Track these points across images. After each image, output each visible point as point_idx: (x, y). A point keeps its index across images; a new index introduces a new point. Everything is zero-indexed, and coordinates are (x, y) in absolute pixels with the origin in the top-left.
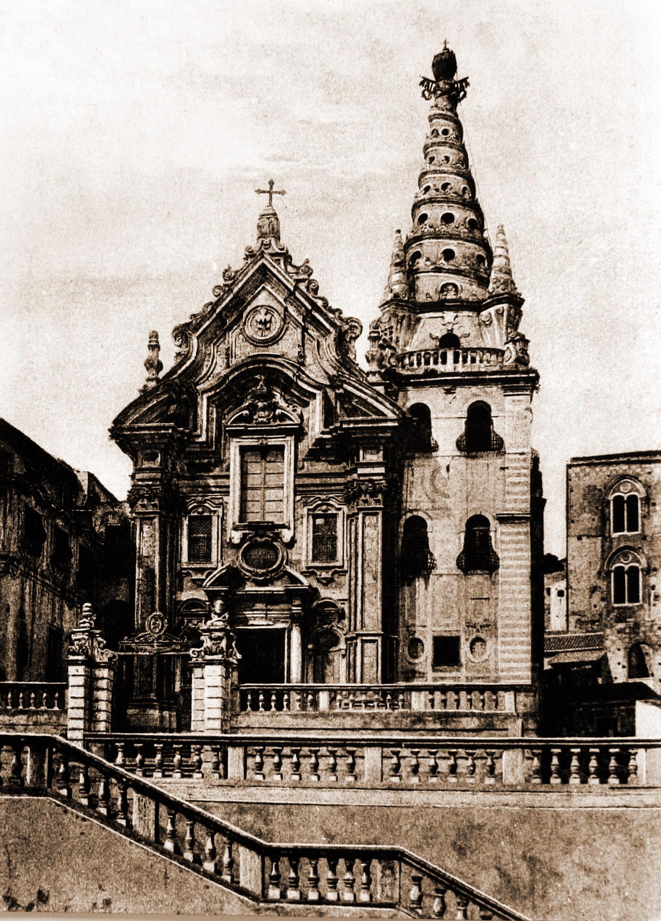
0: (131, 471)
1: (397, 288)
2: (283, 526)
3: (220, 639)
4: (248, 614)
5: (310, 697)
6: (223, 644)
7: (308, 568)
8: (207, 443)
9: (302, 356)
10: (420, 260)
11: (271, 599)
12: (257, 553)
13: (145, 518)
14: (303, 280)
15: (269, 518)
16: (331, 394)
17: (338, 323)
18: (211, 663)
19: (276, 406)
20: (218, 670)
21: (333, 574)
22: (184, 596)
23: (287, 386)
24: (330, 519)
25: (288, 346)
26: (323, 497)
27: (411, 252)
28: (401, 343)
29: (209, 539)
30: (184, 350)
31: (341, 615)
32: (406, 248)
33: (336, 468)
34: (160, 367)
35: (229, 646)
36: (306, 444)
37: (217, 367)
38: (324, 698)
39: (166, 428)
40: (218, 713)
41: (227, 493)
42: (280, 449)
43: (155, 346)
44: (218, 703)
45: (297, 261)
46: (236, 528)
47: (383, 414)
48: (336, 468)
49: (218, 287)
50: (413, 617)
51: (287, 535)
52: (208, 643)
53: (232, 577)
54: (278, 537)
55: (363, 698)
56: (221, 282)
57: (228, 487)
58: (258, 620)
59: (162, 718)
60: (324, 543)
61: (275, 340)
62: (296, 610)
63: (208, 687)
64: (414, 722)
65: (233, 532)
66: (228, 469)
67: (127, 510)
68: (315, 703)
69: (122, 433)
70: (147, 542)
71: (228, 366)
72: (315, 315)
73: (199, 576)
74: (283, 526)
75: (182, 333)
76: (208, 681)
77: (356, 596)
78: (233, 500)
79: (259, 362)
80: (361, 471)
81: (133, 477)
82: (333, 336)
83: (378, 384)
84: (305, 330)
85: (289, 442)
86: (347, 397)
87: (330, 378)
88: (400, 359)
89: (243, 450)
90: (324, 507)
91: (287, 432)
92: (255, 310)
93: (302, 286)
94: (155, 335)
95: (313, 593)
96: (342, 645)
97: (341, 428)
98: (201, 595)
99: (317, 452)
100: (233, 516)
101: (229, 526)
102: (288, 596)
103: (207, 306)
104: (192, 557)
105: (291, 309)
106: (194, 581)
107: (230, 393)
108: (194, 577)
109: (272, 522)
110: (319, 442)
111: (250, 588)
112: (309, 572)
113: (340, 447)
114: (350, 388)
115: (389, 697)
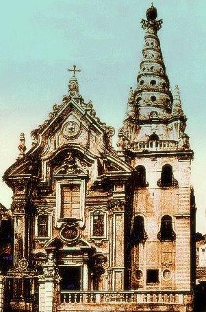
1: (130, 114)
2: (80, 220)
3: (52, 270)
4: (64, 259)
5: (92, 297)
6: (53, 273)
8: (47, 183)
9: (88, 144)
11: (75, 253)
12: (69, 232)
13: (18, 217)
14: (89, 110)
15: (73, 217)
16: (101, 161)
18: (48, 281)
19: (76, 167)
20: (52, 284)
22: (36, 251)
23: (82, 157)
24: (101, 217)
25: (82, 140)
27: (137, 97)
28: (132, 138)
29: (47, 226)
30: (36, 141)
31: (106, 260)
32: (135, 95)
33: (103, 194)
34: (25, 149)
35: (56, 274)
36: (90, 183)
37: (50, 149)
38: (98, 297)
39: (28, 176)
40: (51, 304)
42: (78, 186)
44: (52, 299)
46: (59, 221)
47: (122, 169)
48: (103, 194)
50: (137, 260)
51: (81, 224)
52: (46, 272)
53: (57, 243)
54: (77, 225)
55: (116, 297)
58: (69, 262)
59: (26, 306)
60: (98, 229)
61: (76, 137)
62: (86, 257)
63: (46, 292)
64: (138, 308)
66: (55, 195)
67: (11, 213)
68: (94, 299)
69: (8, 179)
70: (19, 227)
71: (55, 148)
72: (94, 125)
73: (42, 242)
74: (80, 220)
75: (35, 133)
76: (46, 289)
77: (113, 251)
78: (58, 209)
79: (69, 147)
80: (114, 195)
81: (13, 198)
82: (102, 135)
83: (122, 156)
84: (89, 132)
86: (108, 162)
87: (101, 154)
88: (132, 145)
89: (62, 186)
91: (82, 178)
92: (68, 123)
93: (88, 113)
95: (92, 251)
96: (106, 273)
98: (43, 251)
99: (95, 187)
100: (57, 215)
102: (82, 252)
103: (46, 121)
104: (40, 233)
105: (84, 123)
106: (40, 245)
107: (56, 161)
110: (96, 183)
111: (65, 248)
112: (92, 241)
113: (105, 185)
114: (109, 158)
115: (127, 297)
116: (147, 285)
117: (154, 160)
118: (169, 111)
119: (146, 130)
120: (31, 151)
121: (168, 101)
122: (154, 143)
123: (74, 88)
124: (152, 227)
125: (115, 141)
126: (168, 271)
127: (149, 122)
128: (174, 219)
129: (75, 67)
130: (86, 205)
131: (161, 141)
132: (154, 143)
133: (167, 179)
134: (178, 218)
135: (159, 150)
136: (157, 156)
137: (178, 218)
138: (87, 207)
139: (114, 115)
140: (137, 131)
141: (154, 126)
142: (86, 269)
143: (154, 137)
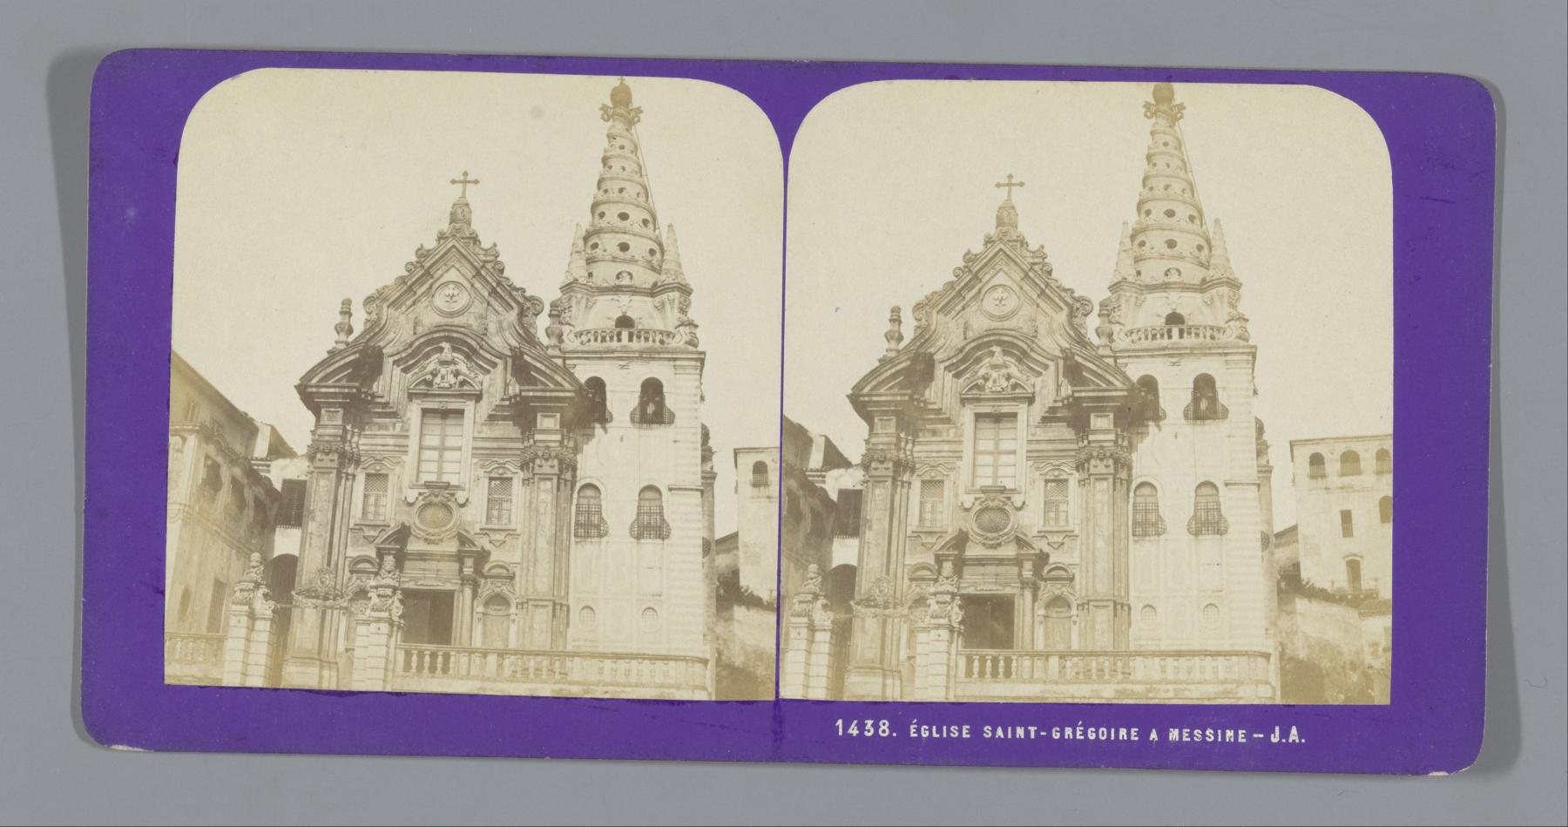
2: (458, 487)
15: (446, 478)
17: (521, 300)
24: (506, 481)
34: (350, 331)
51: (461, 496)
56: (414, 259)
72: (501, 290)
80: (537, 437)
87: (512, 349)
100: (408, 475)
117: (622, 367)
118: (657, 270)
122: (625, 335)
123: (460, 216)
124: (619, 510)
125: (542, 322)
128: (664, 491)
130: (474, 455)
132: (625, 335)
133: (652, 406)
143: (625, 322)
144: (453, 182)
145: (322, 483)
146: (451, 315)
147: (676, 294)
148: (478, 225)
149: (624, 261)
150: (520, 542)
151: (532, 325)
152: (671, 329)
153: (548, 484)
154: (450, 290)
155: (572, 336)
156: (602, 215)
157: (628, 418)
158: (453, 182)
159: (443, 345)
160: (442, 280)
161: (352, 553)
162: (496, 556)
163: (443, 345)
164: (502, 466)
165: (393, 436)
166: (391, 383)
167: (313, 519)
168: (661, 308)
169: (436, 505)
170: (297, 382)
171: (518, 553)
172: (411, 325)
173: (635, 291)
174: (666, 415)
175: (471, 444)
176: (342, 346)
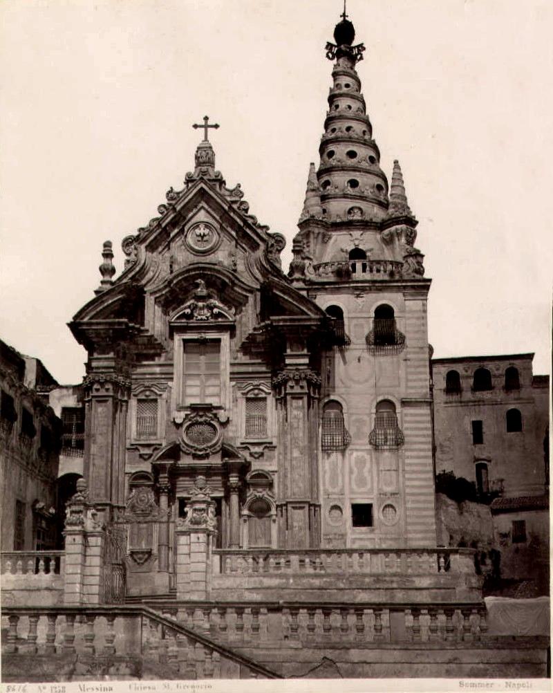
0: (86, 361)
2: (220, 408)
7: (242, 444)
10: (328, 187)
15: (208, 401)
17: (265, 237)
21: (264, 449)
26: (256, 383)
27: (323, 181)
28: (317, 254)
34: (113, 271)
41: (172, 379)
42: (219, 341)
43: (108, 255)
45: (230, 185)
46: (180, 409)
49: (164, 206)
51: (222, 416)
56: (165, 202)
57: (172, 374)
65: (176, 412)
71: (172, 272)
72: (245, 231)
85: (225, 337)
89: (185, 341)
90: (256, 391)
92: (197, 225)
94: (107, 245)
95: (245, 467)
96: (273, 511)
97: (271, 325)
101: (173, 406)
107: (172, 298)
108: (142, 452)
109: (211, 404)
116: (354, 532)
117: (358, 296)
118: (384, 205)
119: (342, 242)
120: (125, 275)
121: (379, 187)
122: (359, 266)
123: (205, 157)
126: (392, 506)
127: (347, 225)
128: (398, 405)
129: (206, 118)
130: (231, 379)
131: (372, 262)
132: (359, 266)
134: (405, 403)
135: (367, 276)
136: (363, 289)
137: (405, 403)
138: (234, 383)
139: (278, 205)
140: (325, 240)
141: (356, 233)
142: (234, 498)
144: (196, 126)
145: (100, 409)
146: (204, 253)
147: (403, 226)
148: (222, 166)
149: (354, 197)
150: (276, 453)
151: (279, 261)
152: (399, 259)
153: (300, 402)
154: (202, 230)
155: (311, 269)
156: (331, 154)
157: (364, 340)
158: (196, 126)
159: (198, 281)
160: (193, 221)
161: (131, 469)
162: (256, 466)
163: (198, 281)
164: (257, 387)
165: (160, 365)
166: (155, 320)
167: (95, 442)
168: (389, 241)
169: (201, 423)
170: (70, 320)
171: (275, 461)
172: (168, 263)
173: (366, 225)
174: (397, 335)
175: (229, 369)
176: (108, 287)
